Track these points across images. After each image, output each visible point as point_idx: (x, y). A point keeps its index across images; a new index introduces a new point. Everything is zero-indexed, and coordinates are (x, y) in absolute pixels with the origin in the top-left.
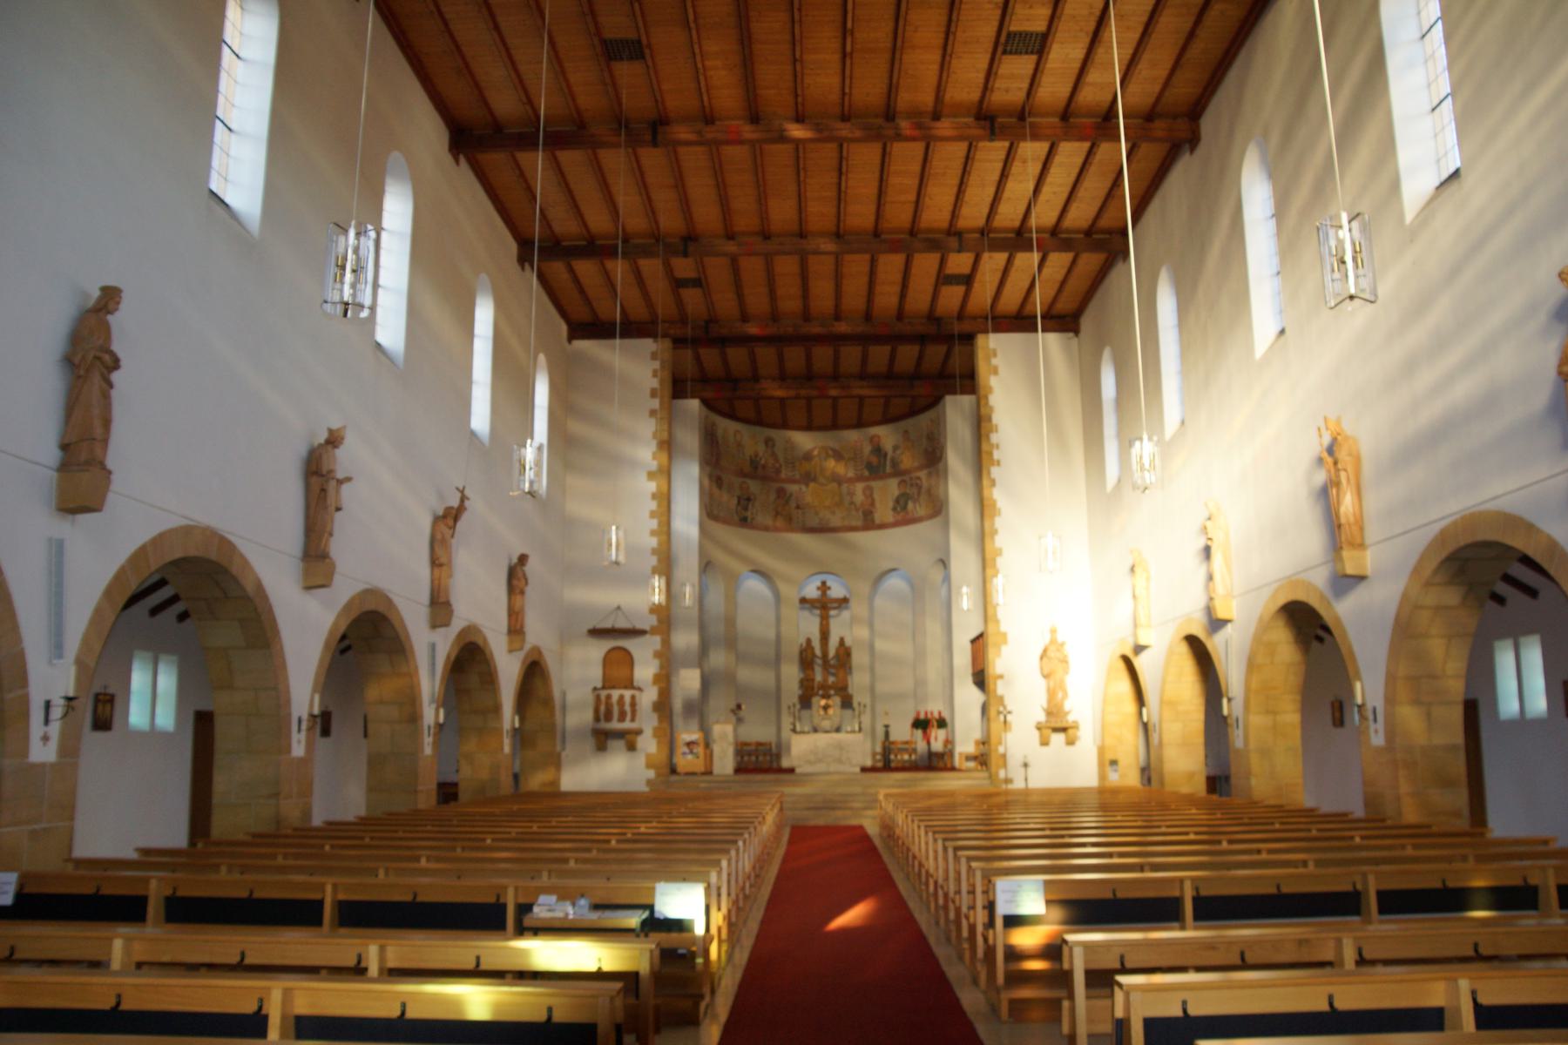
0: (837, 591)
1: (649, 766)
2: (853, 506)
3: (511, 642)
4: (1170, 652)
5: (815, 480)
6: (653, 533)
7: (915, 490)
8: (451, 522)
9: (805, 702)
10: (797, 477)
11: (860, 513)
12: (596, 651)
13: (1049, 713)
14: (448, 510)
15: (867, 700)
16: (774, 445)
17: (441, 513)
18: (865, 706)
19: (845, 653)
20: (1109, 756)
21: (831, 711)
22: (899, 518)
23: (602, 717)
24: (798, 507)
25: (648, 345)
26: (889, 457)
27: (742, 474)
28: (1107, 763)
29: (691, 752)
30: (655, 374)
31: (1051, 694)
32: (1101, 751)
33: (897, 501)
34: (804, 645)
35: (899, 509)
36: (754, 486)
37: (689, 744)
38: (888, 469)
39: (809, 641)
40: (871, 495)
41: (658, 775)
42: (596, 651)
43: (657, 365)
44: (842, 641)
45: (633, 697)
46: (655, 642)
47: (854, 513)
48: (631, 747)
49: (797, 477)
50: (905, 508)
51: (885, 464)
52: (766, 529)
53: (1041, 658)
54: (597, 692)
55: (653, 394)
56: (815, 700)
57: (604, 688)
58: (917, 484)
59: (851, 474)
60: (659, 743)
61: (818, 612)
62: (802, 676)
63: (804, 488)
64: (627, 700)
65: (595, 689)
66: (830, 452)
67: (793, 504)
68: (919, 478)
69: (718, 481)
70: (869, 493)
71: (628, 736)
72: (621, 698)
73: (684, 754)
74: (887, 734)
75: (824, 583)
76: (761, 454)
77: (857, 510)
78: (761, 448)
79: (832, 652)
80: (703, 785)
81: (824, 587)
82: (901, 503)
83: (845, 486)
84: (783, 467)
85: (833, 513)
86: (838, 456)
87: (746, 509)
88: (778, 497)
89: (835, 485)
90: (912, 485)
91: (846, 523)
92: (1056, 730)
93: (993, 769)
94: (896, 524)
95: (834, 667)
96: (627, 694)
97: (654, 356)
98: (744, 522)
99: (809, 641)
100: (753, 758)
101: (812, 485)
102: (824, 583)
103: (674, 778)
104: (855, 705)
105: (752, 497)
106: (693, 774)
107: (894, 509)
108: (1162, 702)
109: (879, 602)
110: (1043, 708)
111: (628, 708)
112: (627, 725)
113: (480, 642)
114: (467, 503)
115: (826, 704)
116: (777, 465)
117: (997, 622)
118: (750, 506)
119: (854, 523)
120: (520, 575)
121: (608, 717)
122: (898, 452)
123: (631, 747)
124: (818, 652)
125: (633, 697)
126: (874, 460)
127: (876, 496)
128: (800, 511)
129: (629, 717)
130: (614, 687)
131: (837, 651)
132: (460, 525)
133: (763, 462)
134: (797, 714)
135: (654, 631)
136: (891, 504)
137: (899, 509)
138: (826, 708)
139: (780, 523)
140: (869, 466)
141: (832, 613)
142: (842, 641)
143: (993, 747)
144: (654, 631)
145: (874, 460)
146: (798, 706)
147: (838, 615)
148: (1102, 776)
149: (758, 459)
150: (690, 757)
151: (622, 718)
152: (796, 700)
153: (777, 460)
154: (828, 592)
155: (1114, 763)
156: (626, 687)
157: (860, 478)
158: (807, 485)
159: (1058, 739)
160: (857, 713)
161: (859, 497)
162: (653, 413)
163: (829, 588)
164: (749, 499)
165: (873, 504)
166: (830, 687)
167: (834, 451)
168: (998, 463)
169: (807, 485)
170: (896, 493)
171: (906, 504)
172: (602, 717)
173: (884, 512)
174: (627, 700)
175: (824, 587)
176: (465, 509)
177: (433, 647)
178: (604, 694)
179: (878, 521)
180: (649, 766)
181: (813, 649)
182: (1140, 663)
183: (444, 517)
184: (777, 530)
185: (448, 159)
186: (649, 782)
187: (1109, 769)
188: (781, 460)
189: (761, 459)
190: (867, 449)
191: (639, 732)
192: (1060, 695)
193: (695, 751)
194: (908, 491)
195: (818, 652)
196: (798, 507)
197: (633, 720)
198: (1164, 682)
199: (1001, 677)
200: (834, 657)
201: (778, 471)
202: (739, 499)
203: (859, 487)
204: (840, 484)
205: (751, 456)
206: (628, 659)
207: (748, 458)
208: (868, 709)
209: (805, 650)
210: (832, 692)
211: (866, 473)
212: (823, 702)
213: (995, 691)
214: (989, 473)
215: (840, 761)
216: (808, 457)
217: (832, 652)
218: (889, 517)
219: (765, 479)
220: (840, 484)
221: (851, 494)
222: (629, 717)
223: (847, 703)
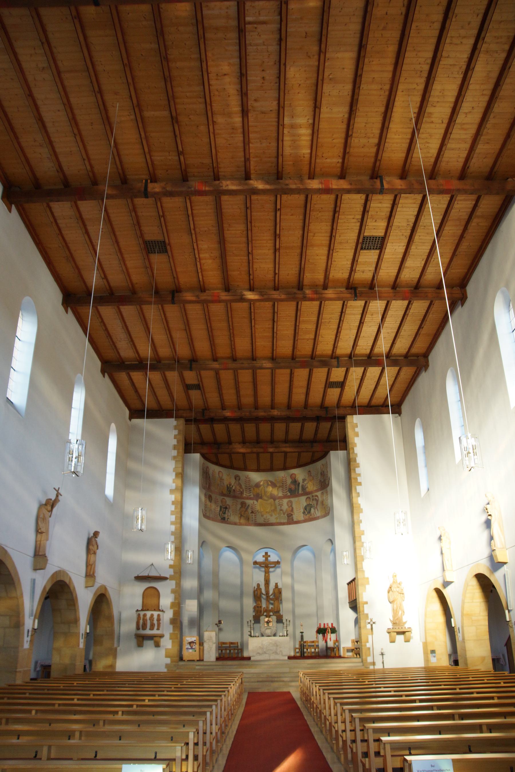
0: (273, 558)
1: (167, 656)
2: (282, 512)
3: (86, 582)
4: (466, 585)
5: (261, 498)
6: (172, 523)
7: (315, 502)
8: (49, 508)
9: (257, 619)
10: (252, 496)
11: (286, 515)
12: (140, 588)
13: (394, 624)
14: (48, 501)
16: (239, 479)
17: (44, 502)
18: (289, 621)
19: (278, 592)
20: (430, 648)
21: (271, 624)
22: (307, 517)
23: (141, 627)
24: (252, 512)
25: (172, 422)
26: (300, 485)
27: (223, 494)
28: (429, 652)
29: (192, 648)
30: (175, 437)
31: (395, 612)
32: (425, 645)
33: (305, 508)
34: (256, 587)
35: (306, 513)
36: (229, 501)
37: (190, 643)
38: (300, 491)
39: (258, 585)
40: (291, 506)
41: (172, 661)
42: (140, 588)
43: (176, 432)
44: (276, 584)
45: (159, 615)
46: (172, 584)
47: (282, 515)
48: (157, 645)
49: (252, 496)
50: (309, 512)
51: (299, 489)
52: (235, 524)
53: (389, 592)
54: (139, 612)
55: (175, 447)
56: (262, 618)
57: (142, 610)
58: (316, 499)
59: (280, 494)
60: (173, 642)
61: (263, 569)
63: (255, 502)
64: (155, 617)
65: (137, 611)
66: (269, 483)
67: (250, 511)
68: (317, 496)
69: (210, 498)
70: (290, 504)
71: (155, 638)
72: (152, 615)
73: (187, 649)
74: (302, 637)
75: (266, 553)
76: (233, 484)
77: (284, 514)
78: (233, 481)
79: (271, 592)
80: (198, 667)
81: (266, 555)
82: (307, 509)
83: (277, 501)
84: (245, 491)
85: (271, 516)
86: (274, 485)
87: (225, 513)
88: (242, 506)
89: (272, 500)
90: (313, 500)
91: (278, 521)
92: (399, 633)
93: (364, 657)
94: (305, 521)
95: (272, 599)
96: (156, 613)
97: (176, 428)
98: (223, 520)
99: (258, 585)
100: (228, 651)
101: (260, 500)
102: (266, 553)
103: (181, 663)
104: (284, 621)
105: (228, 507)
106: (193, 661)
107: (304, 513)
108: (462, 615)
109: (296, 563)
110: (390, 620)
111: (155, 622)
112: (155, 632)
113: (67, 581)
114: (60, 497)
115: (268, 620)
116: (241, 490)
117: (363, 571)
118: (227, 512)
119: (282, 521)
120: (94, 543)
121: (144, 627)
122: (305, 483)
123: (157, 645)
124: (263, 591)
125: (159, 615)
126: (293, 487)
127: (294, 506)
128: (253, 514)
129: (156, 627)
130: (148, 610)
131: (274, 593)
132: (55, 510)
133: (234, 488)
134: (252, 626)
135: (172, 578)
136: (302, 510)
137: (306, 513)
138: (268, 622)
139: (243, 521)
140: (290, 490)
141: (271, 570)
142: (276, 584)
143: (363, 644)
144: (172, 578)
145: (293, 487)
146: (253, 622)
147: (274, 571)
148: (427, 660)
149: (231, 487)
150: (191, 651)
151: (152, 628)
152: (251, 618)
153: (241, 486)
154: (269, 558)
155: (433, 652)
156: (155, 610)
157: (285, 497)
158: (257, 501)
159: (400, 638)
160: (285, 625)
161: (285, 507)
162: (174, 458)
163: (269, 556)
164: (226, 508)
165: (292, 510)
166: (270, 611)
167: (271, 482)
168: (360, 484)
169: (257, 501)
170: (305, 504)
171: (310, 510)
172: (141, 627)
173: (298, 515)
174: (155, 617)
175: (266, 555)
176: (59, 501)
177: (34, 582)
178: (142, 613)
179: (295, 520)
180: (167, 656)
181: (261, 589)
182: (447, 592)
183: (46, 505)
184: (240, 524)
185: (61, 309)
186: (167, 666)
187: (430, 655)
188: (243, 487)
189: (232, 486)
190: (289, 481)
191: (162, 636)
192: (400, 612)
193: (194, 647)
194: (311, 503)
195: (263, 591)
196: (252, 512)
197: (158, 629)
198: (463, 602)
199: (366, 603)
200: (272, 595)
201: (242, 493)
202: (221, 507)
203: (285, 501)
204: (275, 500)
205: (227, 485)
206: (157, 594)
207: (226, 486)
209: (257, 590)
210: (271, 614)
211: (289, 494)
212: (266, 619)
213: (363, 611)
214: (356, 489)
215: (276, 653)
216: (257, 485)
217: (271, 592)
218: (301, 517)
219: (235, 497)
220: (275, 500)
221: (281, 505)
222: (156, 627)
223: (280, 620)
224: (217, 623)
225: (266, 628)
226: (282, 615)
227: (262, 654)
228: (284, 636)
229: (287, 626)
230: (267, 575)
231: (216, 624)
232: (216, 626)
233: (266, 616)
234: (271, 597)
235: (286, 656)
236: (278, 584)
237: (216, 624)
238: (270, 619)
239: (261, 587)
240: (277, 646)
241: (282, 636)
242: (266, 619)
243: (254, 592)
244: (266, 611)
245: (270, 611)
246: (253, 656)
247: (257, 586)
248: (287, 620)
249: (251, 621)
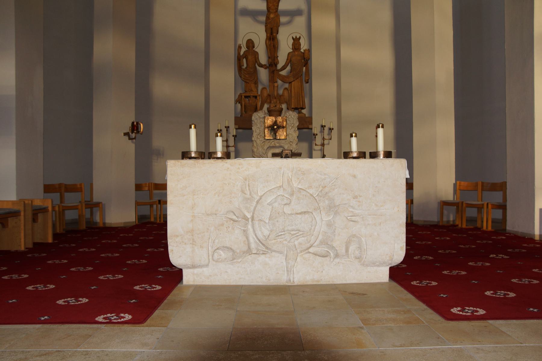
15: (331, 121)
18: (331, 129)
21: (282, 134)
34: (243, 50)
56: (257, 117)
62: (240, 91)
79: (282, 59)
95: (284, 79)
99: (250, 44)
104: (316, 128)
115: (275, 123)
124: (263, 59)
131: (289, 60)
138: (274, 129)
142: (296, 41)
146: (233, 131)
147: (289, 23)
160: (318, 140)
181: (256, 54)
195: (263, 59)
200: (284, 68)
208: (335, 133)
209: (245, 56)
212: (270, 121)
224: (127, 130)
225: (267, 145)
226: (311, 118)
227: (249, 251)
228: (374, 155)
229: (323, 145)
230: (272, 16)
231: (125, 134)
232: (127, 137)
233: (270, 113)
234: (283, 73)
235: (382, 264)
236: (302, 41)
237: (125, 134)
238: (280, 119)
239: (257, 49)
240: (333, 209)
241: (362, 155)
242: (270, 121)
243: (239, 59)
244: (270, 98)
245: (281, 101)
246: (194, 267)
247: (248, 47)
248: (323, 127)
249: (227, 128)
